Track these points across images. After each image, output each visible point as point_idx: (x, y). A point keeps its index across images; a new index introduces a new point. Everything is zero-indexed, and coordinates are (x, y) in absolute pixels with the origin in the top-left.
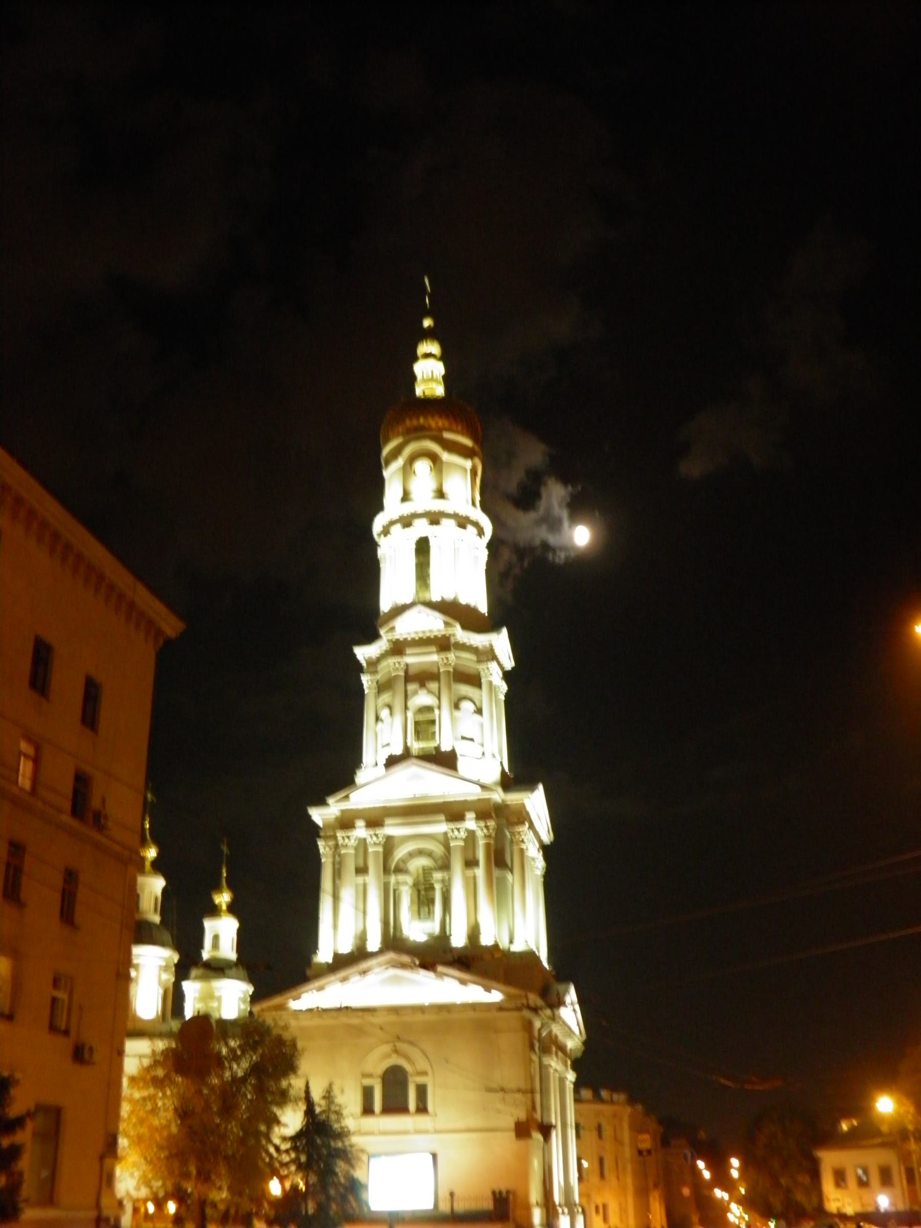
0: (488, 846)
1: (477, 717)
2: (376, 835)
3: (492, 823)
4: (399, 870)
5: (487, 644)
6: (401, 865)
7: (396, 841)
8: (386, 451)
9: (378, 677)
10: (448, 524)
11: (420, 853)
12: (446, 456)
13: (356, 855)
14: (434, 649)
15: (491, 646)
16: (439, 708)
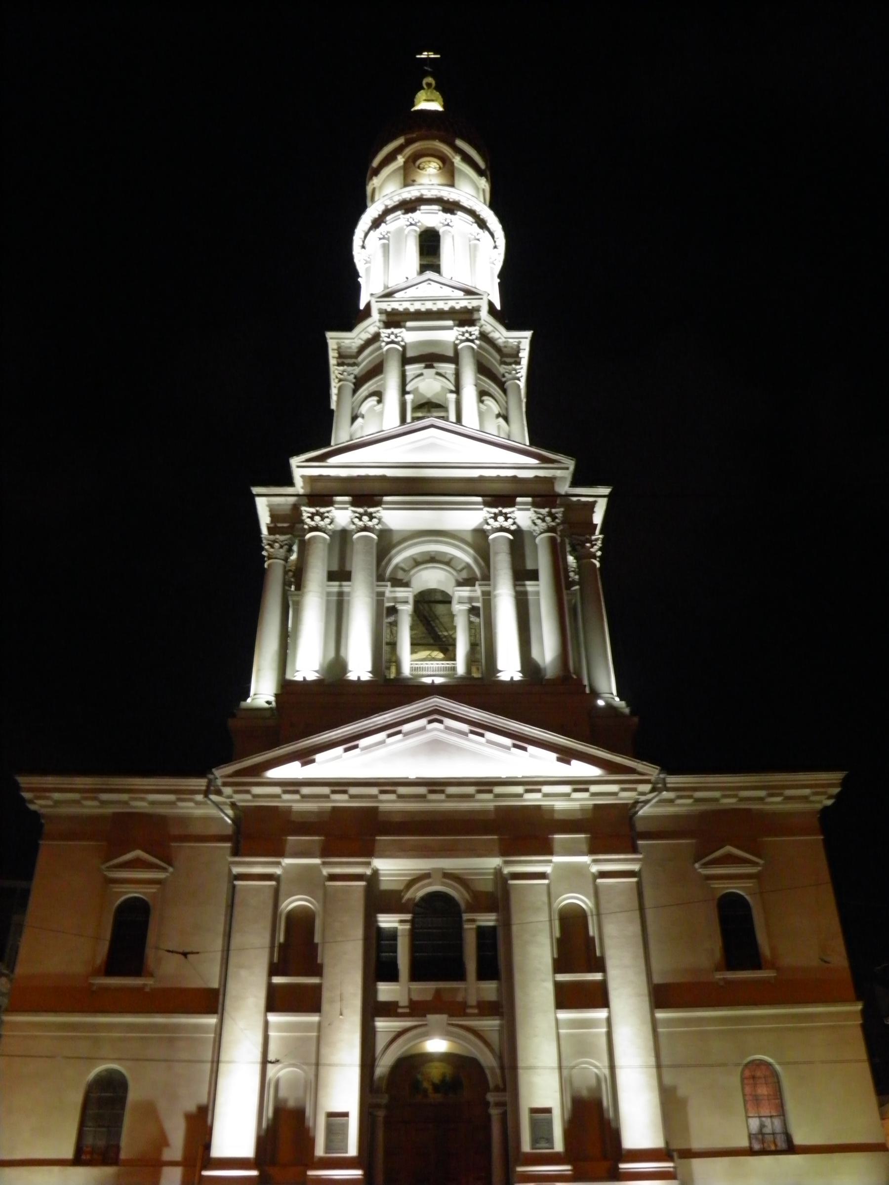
0: (552, 541)
1: (501, 420)
2: (371, 517)
3: (558, 511)
4: (398, 583)
5: (513, 342)
6: (400, 575)
7: (396, 539)
8: (375, 163)
9: (356, 370)
10: (461, 222)
11: (432, 559)
12: (457, 160)
13: (330, 546)
14: (450, 323)
15: (518, 347)
16: (457, 391)
